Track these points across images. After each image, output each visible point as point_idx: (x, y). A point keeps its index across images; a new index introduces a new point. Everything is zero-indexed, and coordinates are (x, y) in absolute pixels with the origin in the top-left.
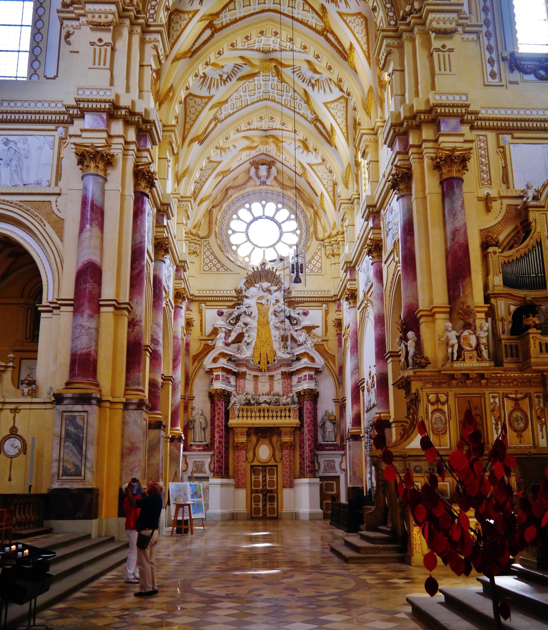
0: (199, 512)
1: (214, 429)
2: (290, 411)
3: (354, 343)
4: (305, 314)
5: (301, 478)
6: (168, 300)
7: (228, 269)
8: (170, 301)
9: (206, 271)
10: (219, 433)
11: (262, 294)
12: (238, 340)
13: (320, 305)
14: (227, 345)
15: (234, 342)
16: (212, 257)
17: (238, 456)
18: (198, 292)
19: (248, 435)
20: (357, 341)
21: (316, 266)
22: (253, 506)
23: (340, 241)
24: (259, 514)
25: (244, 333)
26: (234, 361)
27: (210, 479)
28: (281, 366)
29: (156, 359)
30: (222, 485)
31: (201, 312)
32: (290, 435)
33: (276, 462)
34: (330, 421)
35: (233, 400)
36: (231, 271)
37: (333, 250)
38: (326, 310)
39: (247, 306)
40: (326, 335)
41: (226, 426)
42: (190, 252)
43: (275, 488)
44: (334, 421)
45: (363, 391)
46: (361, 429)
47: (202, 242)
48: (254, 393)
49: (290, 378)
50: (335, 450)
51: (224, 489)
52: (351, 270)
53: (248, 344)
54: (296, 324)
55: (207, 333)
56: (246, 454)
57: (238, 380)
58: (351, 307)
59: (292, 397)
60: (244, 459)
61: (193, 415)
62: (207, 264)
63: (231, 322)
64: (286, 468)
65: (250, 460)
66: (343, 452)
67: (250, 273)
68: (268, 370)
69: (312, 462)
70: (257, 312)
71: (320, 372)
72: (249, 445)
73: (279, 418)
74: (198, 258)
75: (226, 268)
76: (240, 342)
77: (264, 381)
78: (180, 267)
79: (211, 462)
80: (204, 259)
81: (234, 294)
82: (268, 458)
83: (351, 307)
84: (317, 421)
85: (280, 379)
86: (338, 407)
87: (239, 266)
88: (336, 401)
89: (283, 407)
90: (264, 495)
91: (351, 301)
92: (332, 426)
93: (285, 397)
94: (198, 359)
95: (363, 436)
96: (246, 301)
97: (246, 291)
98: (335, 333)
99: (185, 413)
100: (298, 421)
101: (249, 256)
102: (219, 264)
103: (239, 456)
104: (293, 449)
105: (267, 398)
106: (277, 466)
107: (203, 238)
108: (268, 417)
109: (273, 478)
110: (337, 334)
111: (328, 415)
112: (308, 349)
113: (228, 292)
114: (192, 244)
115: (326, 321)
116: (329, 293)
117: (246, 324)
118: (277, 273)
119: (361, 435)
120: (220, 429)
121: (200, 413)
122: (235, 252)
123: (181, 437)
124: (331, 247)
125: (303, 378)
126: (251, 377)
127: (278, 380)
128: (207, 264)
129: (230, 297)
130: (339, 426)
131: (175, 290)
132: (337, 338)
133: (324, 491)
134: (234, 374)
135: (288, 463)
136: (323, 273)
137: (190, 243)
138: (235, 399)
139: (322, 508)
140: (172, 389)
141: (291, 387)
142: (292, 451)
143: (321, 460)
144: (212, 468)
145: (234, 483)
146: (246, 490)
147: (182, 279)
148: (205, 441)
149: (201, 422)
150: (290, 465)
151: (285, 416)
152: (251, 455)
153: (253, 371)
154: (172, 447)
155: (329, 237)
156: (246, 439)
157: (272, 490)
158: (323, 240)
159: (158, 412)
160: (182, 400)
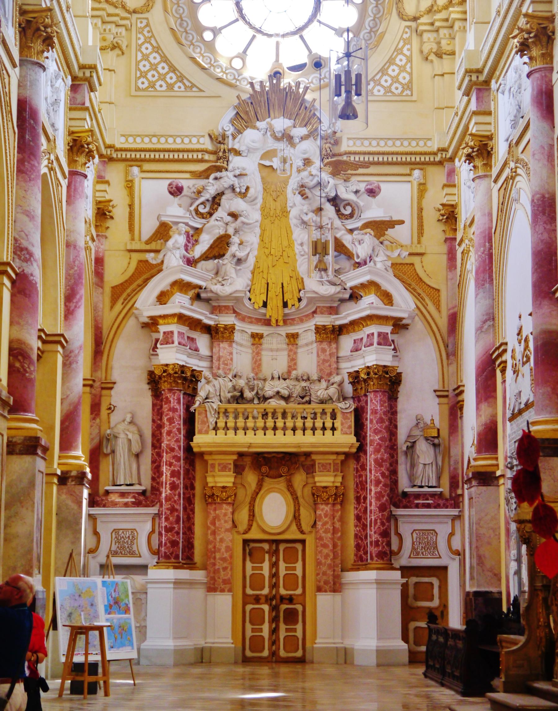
0: (123, 645)
1: (160, 455)
2: (334, 416)
3: (484, 261)
4: (372, 192)
5: (358, 569)
6: (52, 157)
7: (193, 85)
8: (57, 159)
9: (143, 90)
10: (171, 465)
11: (272, 144)
12: (215, 252)
13: (408, 172)
14: (191, 262)
15: (206, 257)
16: (155, 58)
17: (214, 519)
18: (123, 139)
19: (238, 469)
20: (491, 256)
21: (398, 81)
22: (249, 633)
23: (455, 20)
24: (262, 650)
25: (229, 236)
26: (208, 300)
27: (150, 571)
28: (315, 312)
29: (25, 295)
30: (178, 583)
31: (130, 186)
32: (335, 470)
33: (302, 532)
34: (427, 439)
35: (203, 389)
36: (201, 90)
37: (439, 43)
38: (420, 184)
39: (237, 172)
40: (419, 242)
41: (188, 449)
42: (104, 44)
43: (299, 591)
44: (436, 441)
45: (503, 371)
46: (497, 459)
47: (134, 21)
48: (252, 375)
49: (336, 340)
50: (437, 506)
51: (183, 592)
52: (479, 90)
53: (239, 261)
54: (351, 216)
55: (146, 235)
56: (233, 513)
57: (215, 344)
58: (479, 177)
59: (341, 384)
60: (229, 525)
61: (112, 424)
62: (144, 75)
63: (201, 209)
64: (325, 546)
65: (243, 526)
66: (454, 512)
67: (245, 96)
69: (385, 534)
70: (260, 187)
71: (405, 327)
72: (241, 493)
73: (309, 432)
74: (123, 59)
75: (188, 84)
76: (221, 256)
77: (274, 346)
78: (81, 79)
79: (153, 531)
80: (138, 63)
81: (208, 145)
82: (284, 522)
83: (479, 177)
84: (396, 440)
85: (312, 343)
86: (446, 409)
87: (219, 79)
88: (440, 394)
89: (318, 408)
90: (275, 609)
91: (479, 162)
92: (431, 450)
93: (324, 384)
94: (124, 295)
95: (503, 476)
96: (235, 162)
97: (234, 138)
98: (442, 237)
99: (94, 419)
100: (352, 439)
101: (243, 55)
102: (171, 74)
103: (216, 518)
104: (342, 503)
105: (282, 387)
106: (303, 542)
107: (135, 12)
109: (294, 569)
110: (446, 240)
111: (421, 425)
112: (377, 274)
113: (194, 140)
114: (108, 26)
115: (420, 210)
116: (429, 143)
117: (234, 216)
118: (309, 97)
119: (498, 473)
120: (174, 457)
121: (128, 419)
122: (210, 46)
123: (84, 474)
124: (435, 35)
125: (365, 340)
126: (247, 337)
127: (307, 345)
128: (144, 75)
129: (198, 151)
130: (447, 453)
131: (71, 133)
132: (444, 249)
133: (410, 600)
134: (208, 329)
135: (329, 535)
136: (414, 98)
137: (104, 22)
138: (208, 388)
139: (405, 638)
140: (64, 365)
141: (338, 362)
142: (338, 507)
143: (405, 529)
144: (155, 546)
146: (233, 596)
147: (87, 109)
148: (140, 484)
149: (130, 441)
150: (332, 539)
151: (324, 428)
152: (243, 516)
153: (251, 322)
154: (64, 497)
155: (430, 11)
156: (232, 480)
157: (291, 595)
158: (415, 19)
159: (30, 416)
160: (88, 389)
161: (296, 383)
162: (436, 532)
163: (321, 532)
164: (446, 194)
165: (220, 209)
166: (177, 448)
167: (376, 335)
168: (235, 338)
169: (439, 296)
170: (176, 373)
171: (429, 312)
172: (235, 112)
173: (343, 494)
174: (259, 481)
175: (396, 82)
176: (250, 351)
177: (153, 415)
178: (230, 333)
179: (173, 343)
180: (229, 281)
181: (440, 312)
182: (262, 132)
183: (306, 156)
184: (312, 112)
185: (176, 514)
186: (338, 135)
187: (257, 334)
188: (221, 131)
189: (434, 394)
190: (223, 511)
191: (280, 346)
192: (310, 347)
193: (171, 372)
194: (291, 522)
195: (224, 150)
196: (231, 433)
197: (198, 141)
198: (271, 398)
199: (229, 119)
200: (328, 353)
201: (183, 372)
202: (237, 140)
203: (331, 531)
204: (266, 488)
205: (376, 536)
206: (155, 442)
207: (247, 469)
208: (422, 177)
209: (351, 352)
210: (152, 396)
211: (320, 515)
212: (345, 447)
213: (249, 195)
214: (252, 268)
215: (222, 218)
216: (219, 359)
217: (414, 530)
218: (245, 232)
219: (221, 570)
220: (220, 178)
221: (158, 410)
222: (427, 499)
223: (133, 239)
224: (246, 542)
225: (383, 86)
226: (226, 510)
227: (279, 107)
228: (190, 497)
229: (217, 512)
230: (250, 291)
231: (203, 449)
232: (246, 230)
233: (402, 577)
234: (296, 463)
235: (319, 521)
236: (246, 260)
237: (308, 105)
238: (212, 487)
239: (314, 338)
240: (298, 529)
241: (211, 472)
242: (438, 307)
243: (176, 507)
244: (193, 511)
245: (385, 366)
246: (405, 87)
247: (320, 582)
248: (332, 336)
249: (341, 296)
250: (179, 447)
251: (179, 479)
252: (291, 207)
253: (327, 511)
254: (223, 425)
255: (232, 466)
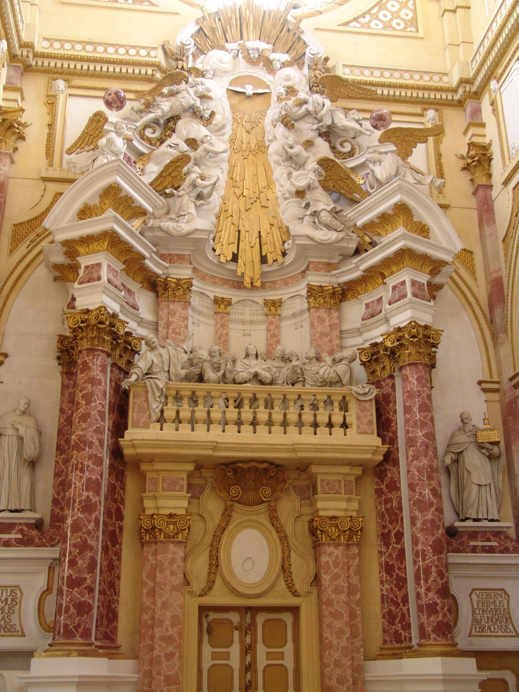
2: (344, 407)
5: (397, 656)
17: (154, 569)
18: (46, 44)
21: (398, 17)
27: (34, 661)
28: (308, 268)
32: (349, 492)
33: (295, 594)
34: (480, 447)
36: (153, 4)
50: (506, 550)
54: (351, 154)
56: (185, 559)
57: (163, 304)
60: (178, 580)
63: (148, 133)
64: (336, 615)
68: (263, 286)
70: (228, 114)
72: (197, 528)
77: (247, 317)
79: (48, 590)
81: (160, 58)
85: (302, 313)
94: (32, 236)
100: (375, 441)
108: (270, 423)
111: (469, 428)
116: (445, 79)
121: (22, 408)
125: (385, 300)
127: (294, 315)
129: (147, 65)
132: (473, 202)
136: (421, 34)
138: (151, 356)
141: (341, 338)
145: (135, 677)
149: (21, 439)
151: (330, 425)
153: (215, 283)
156: (185, 504)
161: (282, 364)
162: (506, 593)
163: (329, 591)
164: (473, 135)
165: (174, 136)
166: (97, 443)
167: (408, 284)
168: (192, 300)
169: (473, 259)
170: (101, 323)
171: (462, 279)
172: (198, 27)
173: (361, 530)
174: (226, 510)
175: (396, 18)
176: (212, 322)
177: (62, 401)
178: (184, 291)
179: (99, 279)
180: (186, 217)
181: (475, 279)
182: (232, 54)
183: (289, 84)
184: (296, 36)
185: (89, 554)
186: (329, 64)
187: (222, 298)
188: (179, 44)
189: (478, 388)
190: (169, 556)
191: (255, 318)
192: (299, 319)
193: (93, 321)
194: (278, 576)
195: (183, 67)
196: (185, 428)
197: (148, 54)
198: (246, 382)
199: (190, 35)
200: (327, 324)
201: (112, 325)
202: (199, 60)
203: (346, 591)
204: (238, 521)
205: (431, 595)
206: (62, 442)
207: (207, 491)
208: (437, 119)
209: (363, 319)
210: (61, 373)
211: (327, 563)
212: (366, 452)
213: (214, 122)
214: (216, 211)
215: (176, 145)
216: (168, 325)
217: (474, 590)
218: (208, 167)
219: (164, 660)
220: (178, 93)
221: (70, 394)
222: (489, 540)
223: (51, 165)
224: (203, 610)
225: (381, 21)
226: (173, 553)
227: (255, 27)
228: (114, 531)
229: (159, 557)
230: (214, 240)
231: (139, 451)
232: (209, 164)
233: (480, 668)
234: (284, 481)
235: (326, 573)
236: (210, 195)
237: (291, 27)
238: (153, 515)
239: (306, 306)
240: (289, 588)
241: (150, 491)
242: (473, 272)
243: (91, 542)
244: (118, 555)
245: (426, 327)
246: (408, 23)
247: (330, 679)
248: (332, 302)
249: (344, 244)
250: (101, 442)
251: (98, 494)
252: (271, 141)
253: (337, 556)
254: (174, 415)
255: (185, 483)
